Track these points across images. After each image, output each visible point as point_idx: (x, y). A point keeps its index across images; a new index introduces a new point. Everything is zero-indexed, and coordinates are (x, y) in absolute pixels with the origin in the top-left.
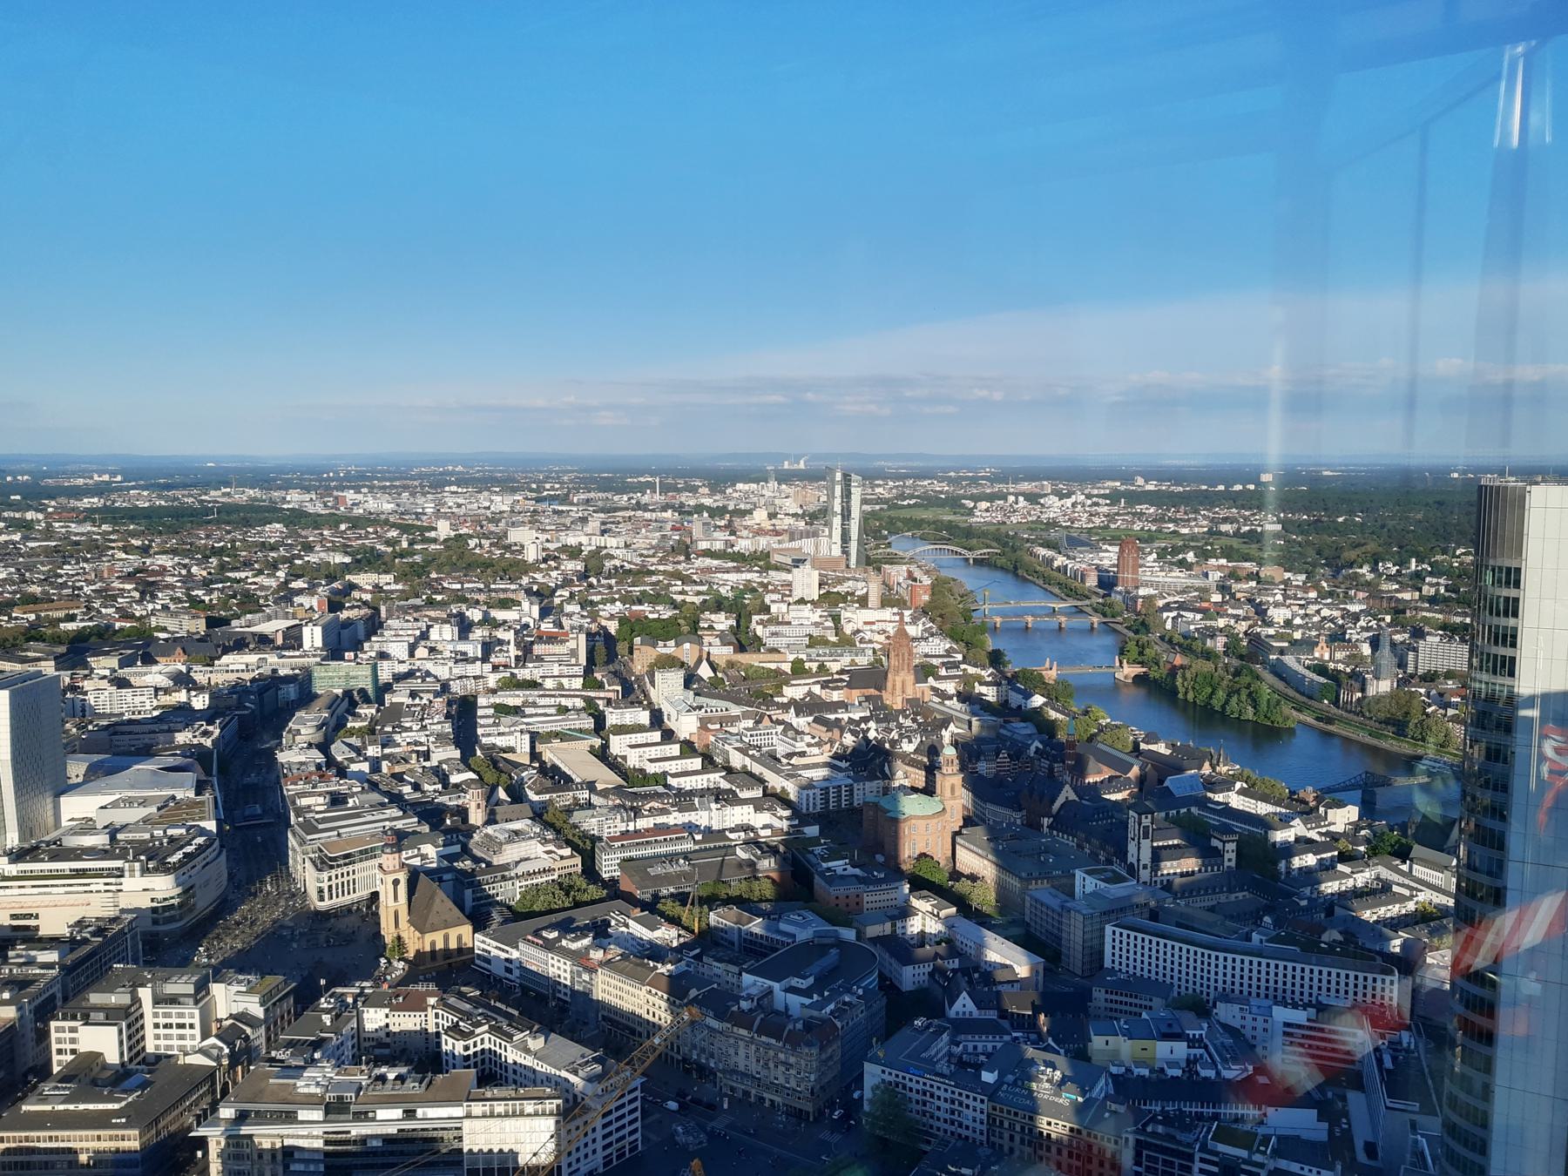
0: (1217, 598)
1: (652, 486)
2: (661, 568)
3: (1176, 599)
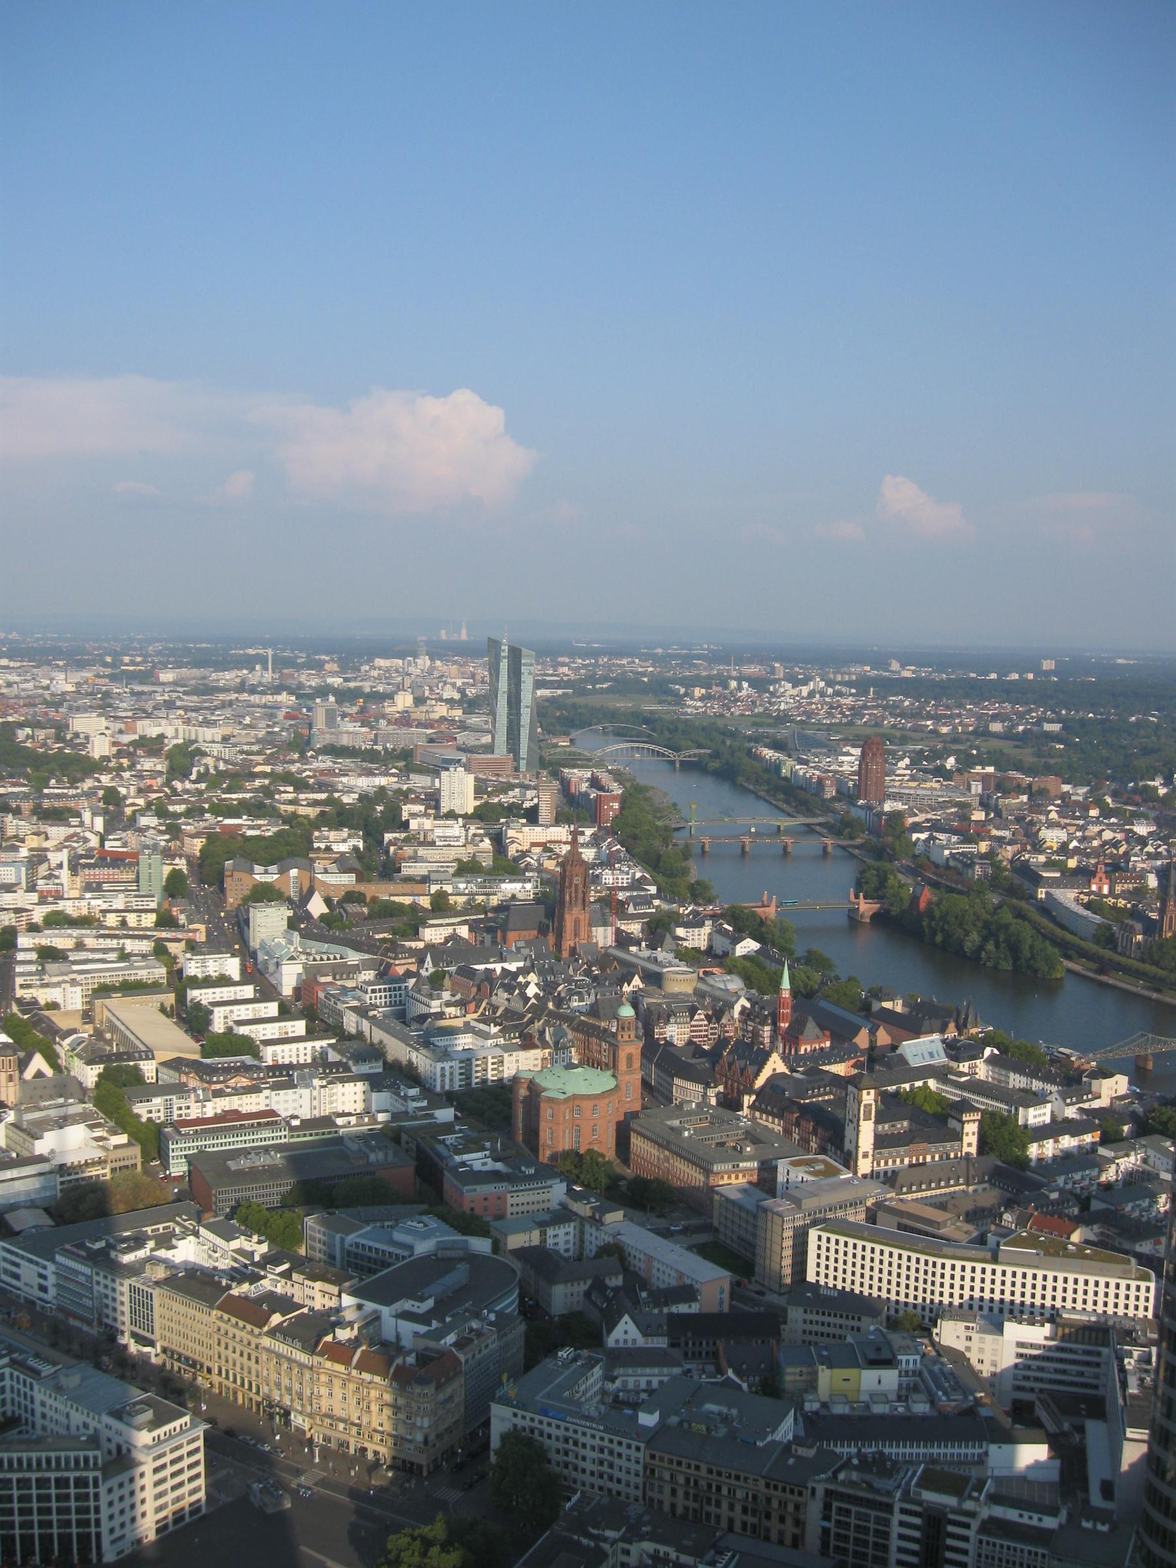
0: (978, 815)
1: (263, 661)
3: (929, 816)
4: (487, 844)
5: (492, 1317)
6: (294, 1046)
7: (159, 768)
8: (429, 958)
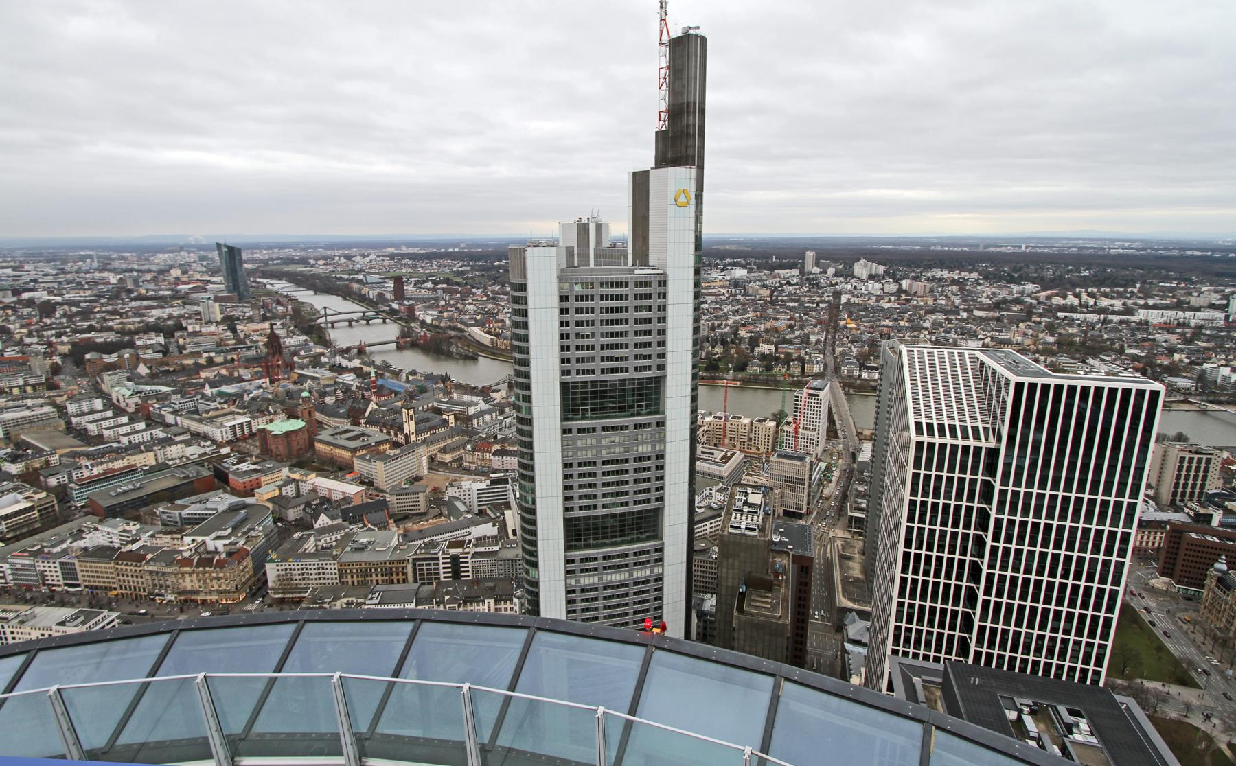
2: (104, 309)
4: (229, 333)
6: (140, 435)
7: (34, 313)
8: (207, 385)
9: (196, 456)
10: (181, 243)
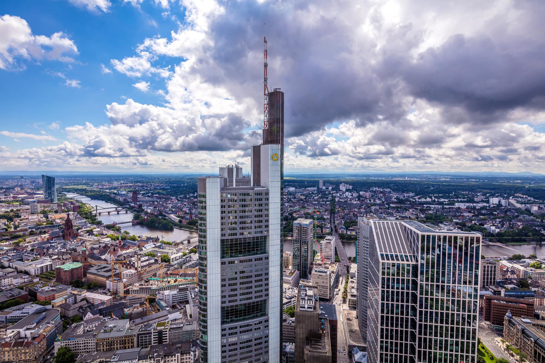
4: (44, 219)
5: (53, 322)
9: (19, 284)
10: (22, 175)
